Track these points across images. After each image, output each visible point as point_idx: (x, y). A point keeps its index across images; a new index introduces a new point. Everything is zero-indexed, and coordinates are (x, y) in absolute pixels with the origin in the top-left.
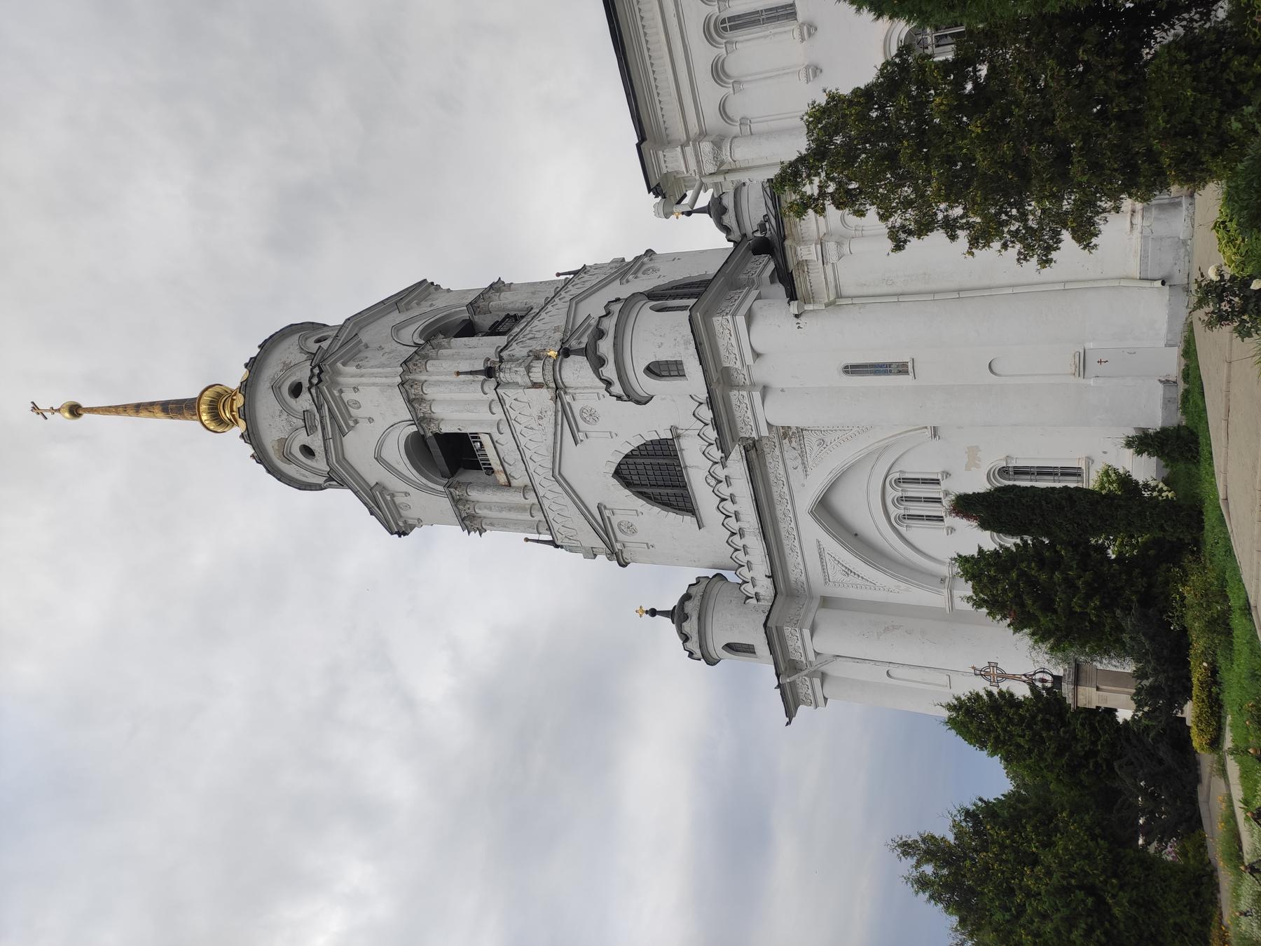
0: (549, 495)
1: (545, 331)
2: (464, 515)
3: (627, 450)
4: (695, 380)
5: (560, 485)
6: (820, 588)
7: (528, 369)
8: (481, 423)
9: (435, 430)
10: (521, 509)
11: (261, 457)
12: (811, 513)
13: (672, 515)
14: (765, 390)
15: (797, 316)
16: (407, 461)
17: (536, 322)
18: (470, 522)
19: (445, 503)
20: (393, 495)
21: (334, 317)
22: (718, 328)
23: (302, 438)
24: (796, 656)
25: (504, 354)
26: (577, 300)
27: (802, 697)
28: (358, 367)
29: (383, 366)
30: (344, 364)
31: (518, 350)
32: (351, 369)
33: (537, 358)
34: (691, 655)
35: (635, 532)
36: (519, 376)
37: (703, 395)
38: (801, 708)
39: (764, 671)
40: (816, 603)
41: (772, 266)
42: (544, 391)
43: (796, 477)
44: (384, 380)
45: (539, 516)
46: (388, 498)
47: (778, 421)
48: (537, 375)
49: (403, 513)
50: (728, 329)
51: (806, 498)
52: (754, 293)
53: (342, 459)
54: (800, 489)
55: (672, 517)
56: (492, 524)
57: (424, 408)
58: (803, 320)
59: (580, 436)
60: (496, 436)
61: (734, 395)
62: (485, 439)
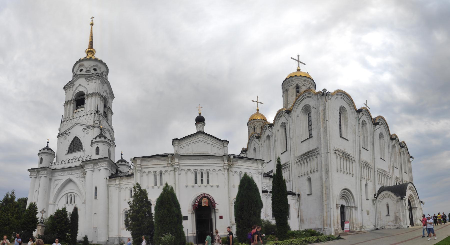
1: (104, 125)
3: (80, 140)
6: (54, 179)
7: (97, 120)
10: (69, 115)
19: (70, 99)
21: (110, 77)
31: (101, 118)
32: (100, 82)
33: (100, 122)
36: (96, 118)
37: (92, 158)
40: (50, 177)
42: (93, 123)
45: (67, 119)
48: (96, 122)
54: (75, 176)
55: (67, 148)
57: (90, 97)
60: (84, 111)
61: (92, 165)
62: (83, 109)
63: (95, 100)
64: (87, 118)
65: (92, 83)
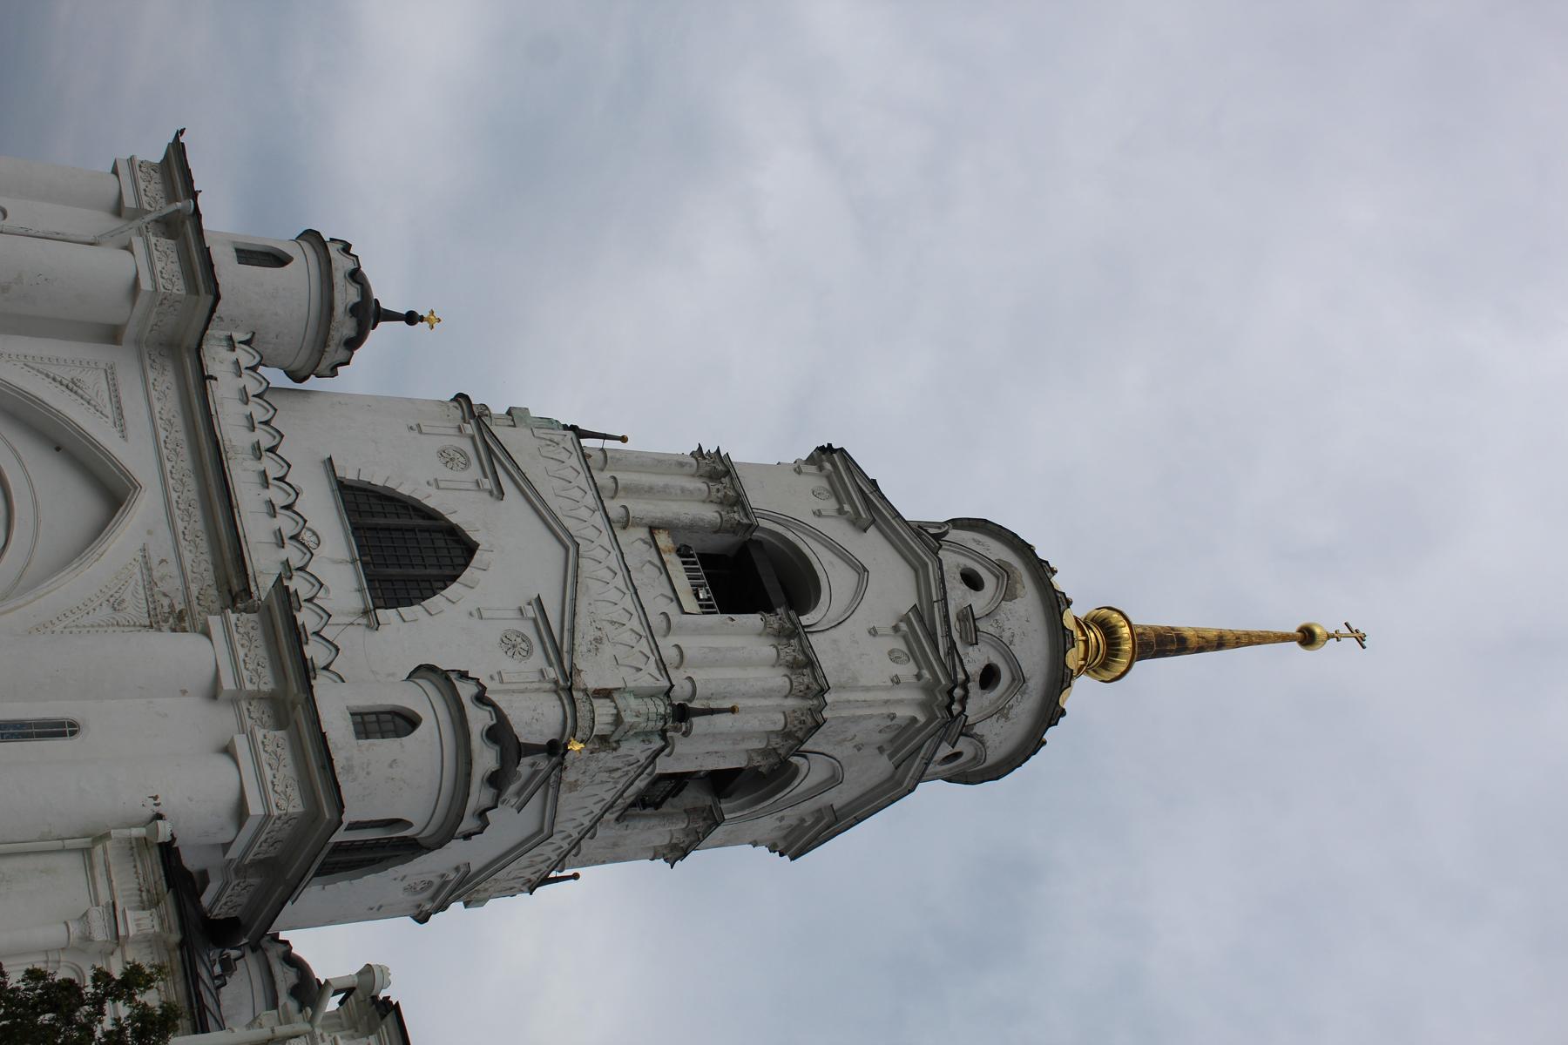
0: (584, 513)
1: (591, 786)
2: (726, 480)
3: (454, 589)
4: (334, 706)
5: (566, 530)
6: (124, 360)
7: (618, 720)
8: (697, 631)
9: (771, 618)
11: (1041, 571)
12: (135, 486)
13: (378, 481)
14: (214, 692)
15: (159, 817)
16: (817, 566)
17: (609, 797)
18: (716, 469)
19: (757, 498)
20: (841, 511)
21: (934, 795)
22: (295, 795)
23: (979, 602)
24: (166, 244)
25: (657, 743)
26: (542, 835)
27: (157, 176)
28: (893, 717)
29: (856, 720)
30: (914, 720)
31: (636, 750)
32: (904, 713)
33: (603, 739)
34: (346, 248)
35: (442, 453)
36: (633, 709)
37: (321, 685)
38: (157, 157)
39: (223, 217)
40: (129, 333)
41: (206, 899)
43: (162, 545)
44: (852, 696)
45: (603, 478)
46: (847, 507)
47: (190, 642)
48: (604, 712)
49: (825, 484)
50: (278, 793)
51: (145, 509)
52: (234, 853)
53: (918, 568)
54: (154, 527)
55: (377, 477)
56: (681, 464)
57: (790, 652)
58: (149, 811)
59: (531, 612)
60: (672, 609)
61: (267, 683)
62: (690, 604)
63: (767, 693)
64: (628, 637)
65: (893, 656)
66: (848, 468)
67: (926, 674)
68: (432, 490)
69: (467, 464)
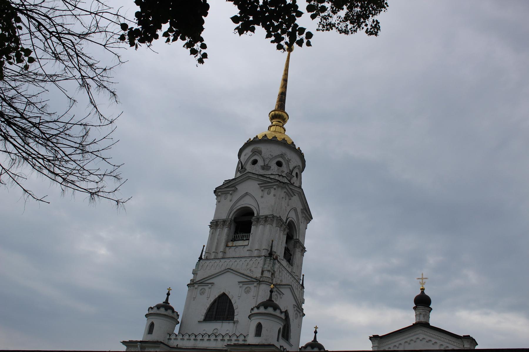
0: (221, 264)
5: (223, 271)
13: (205, 311)
17: (286, 272)
20: (231, 194)
35: (201, 294)
46: (231, 192)
55: (204, 311)
56: (212, 233)
59: (241, 285)
62: (246, 243)
65: (269, 193)
66: (221, 189)
67: (275, 187)
68: (209, 299)
69: (204, 289)
